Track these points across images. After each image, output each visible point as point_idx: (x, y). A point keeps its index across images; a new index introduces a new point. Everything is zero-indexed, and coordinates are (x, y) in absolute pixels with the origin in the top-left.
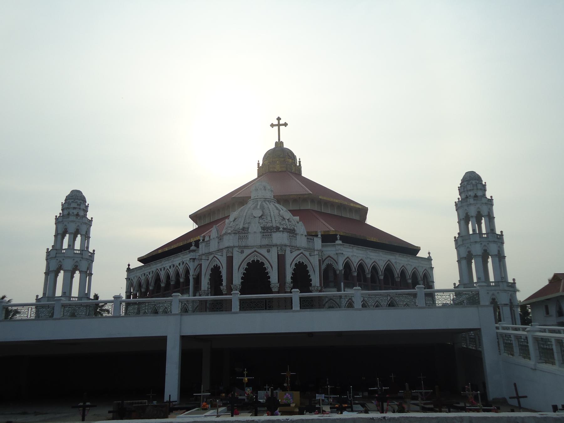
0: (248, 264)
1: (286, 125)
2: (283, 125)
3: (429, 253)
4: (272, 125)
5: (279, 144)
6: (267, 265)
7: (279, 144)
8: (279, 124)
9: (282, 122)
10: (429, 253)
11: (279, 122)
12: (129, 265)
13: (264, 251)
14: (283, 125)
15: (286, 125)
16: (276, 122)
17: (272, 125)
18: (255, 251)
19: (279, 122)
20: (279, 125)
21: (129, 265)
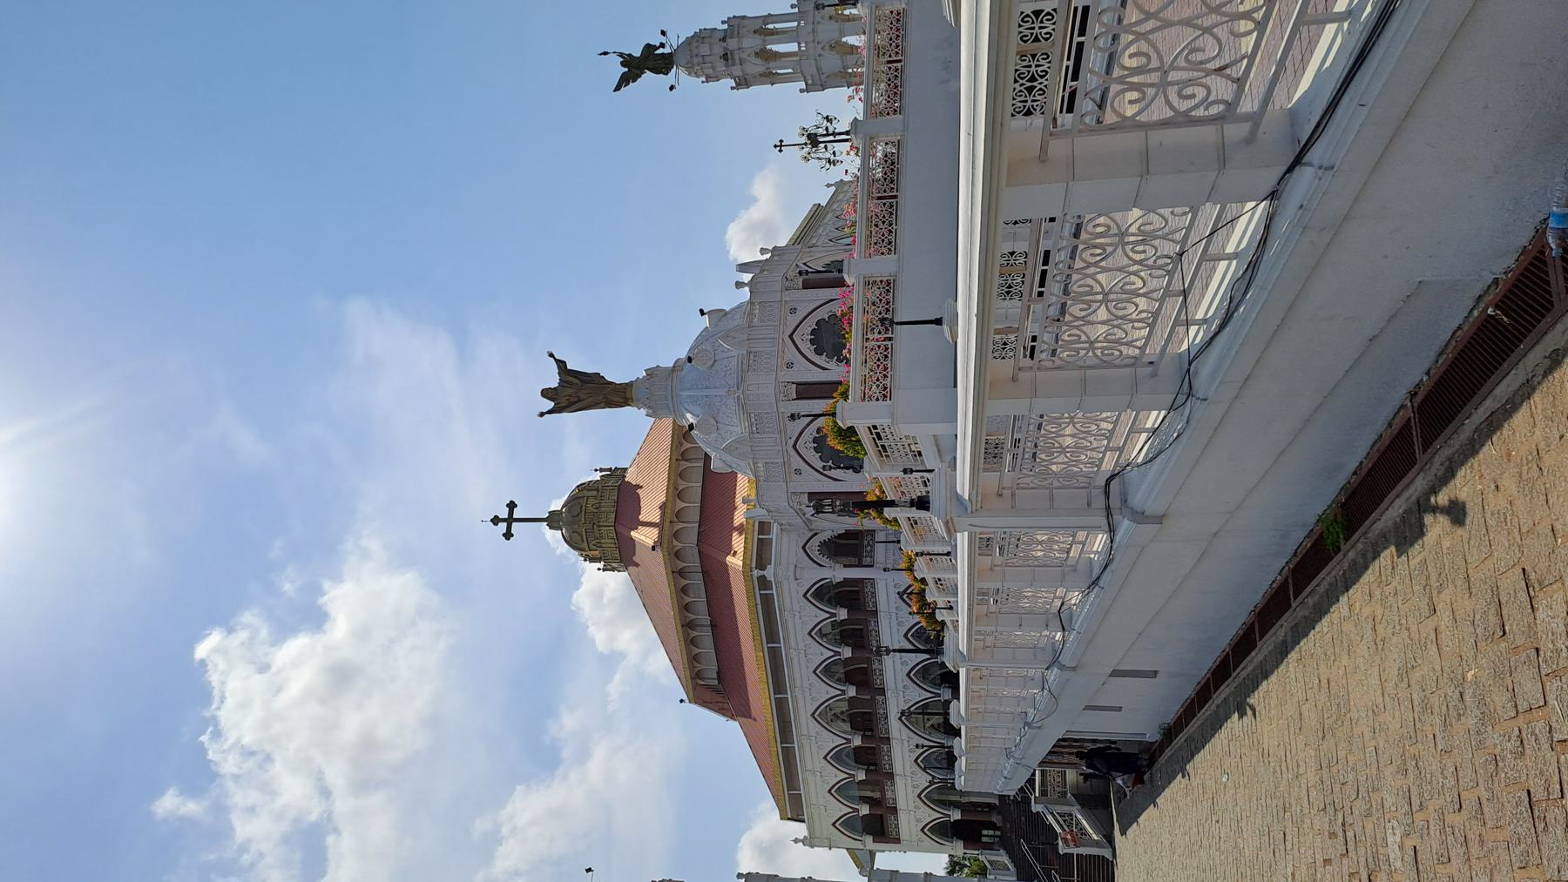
0: (818, 352)
1: (512, 506)
2: (511, 513)
3: (828, 186)
4: (508, 535)
5: (553, 520)
6: (823, 314)
7: (553, 520)
8: (508, 520)
9: (504, 514)
10: (828, 186)
11: (504, 520)
12: (796, 841)
13: (793, 321)
14: (511, 513)
15: (512, 506)
16: (503, 526)
17: (508, 535)
18: (791, 337)
19: (504, 520)
20: (510, 520)
21: (796, 841)
